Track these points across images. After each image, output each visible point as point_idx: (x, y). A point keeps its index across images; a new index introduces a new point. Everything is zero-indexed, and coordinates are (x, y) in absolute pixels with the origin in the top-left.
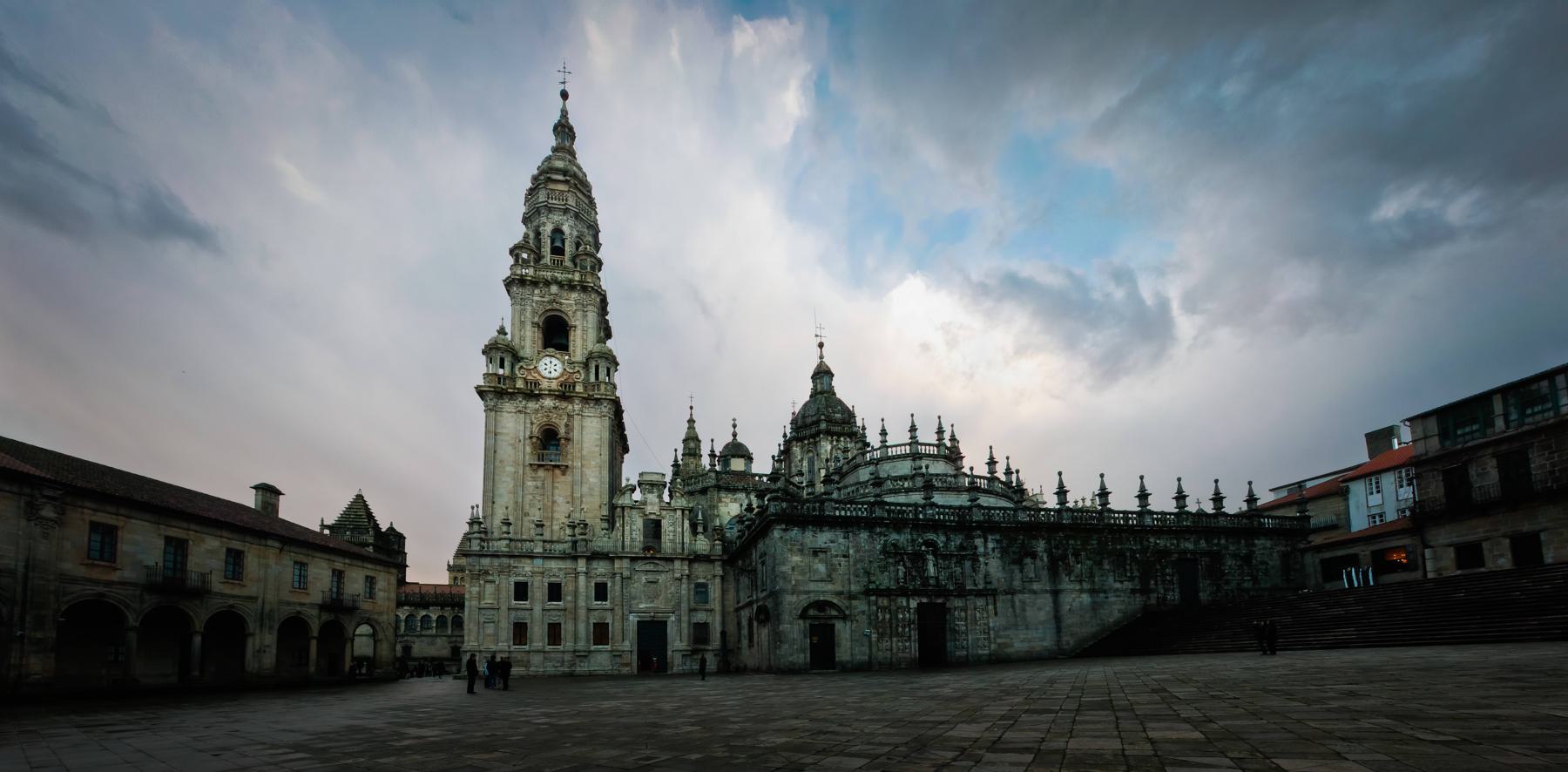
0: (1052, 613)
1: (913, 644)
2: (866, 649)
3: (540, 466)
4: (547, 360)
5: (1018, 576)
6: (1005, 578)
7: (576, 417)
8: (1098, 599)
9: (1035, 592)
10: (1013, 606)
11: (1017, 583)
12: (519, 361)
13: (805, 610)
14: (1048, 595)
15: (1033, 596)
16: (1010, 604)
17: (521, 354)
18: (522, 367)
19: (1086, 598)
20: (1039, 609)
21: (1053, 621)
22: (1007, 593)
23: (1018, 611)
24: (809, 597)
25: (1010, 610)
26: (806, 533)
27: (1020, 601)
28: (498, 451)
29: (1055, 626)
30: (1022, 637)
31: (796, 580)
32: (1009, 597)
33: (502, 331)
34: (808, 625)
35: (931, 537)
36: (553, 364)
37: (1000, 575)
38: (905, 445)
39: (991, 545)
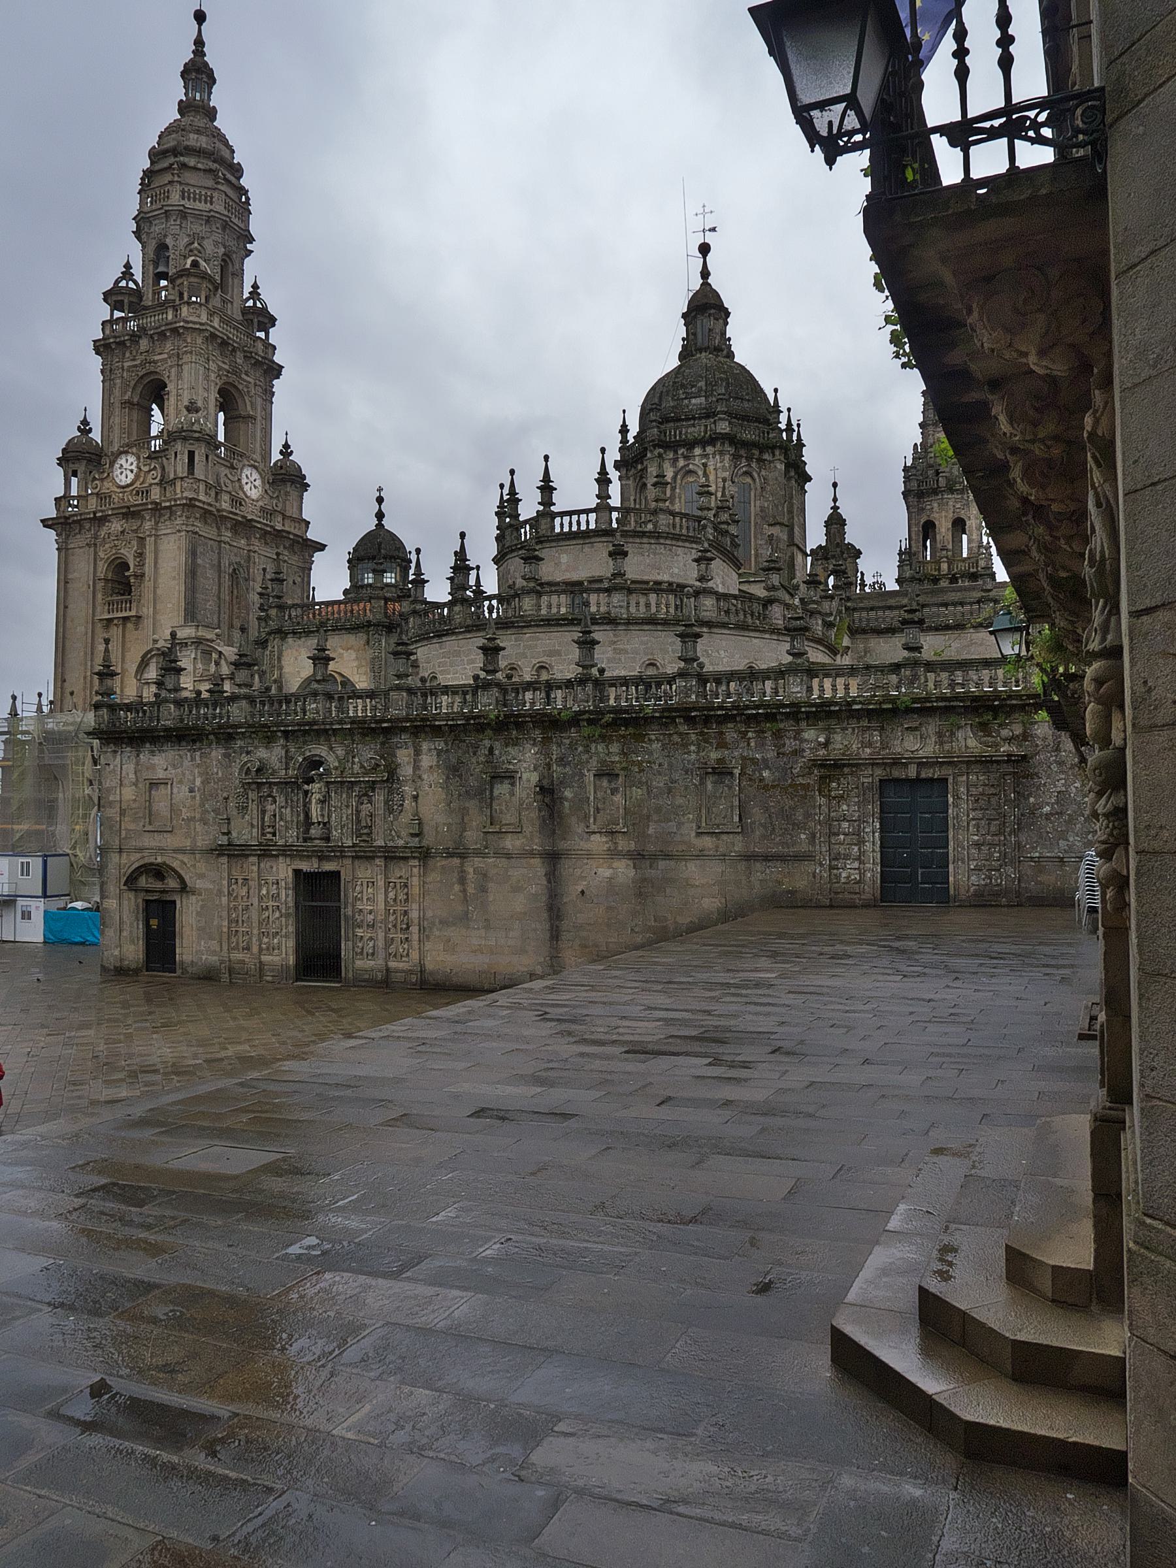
3: (110, 620)
6: (449, 825)
7: (148, 539)
8: (651, 873)
9: (508, 856)
10: (462, 881)
11: (472, 837)
14: (537, 861)
15: (503, 862)
16: (455, 876)
19: (624, 870)
20: (516, 889)
21: (545, 915)
22: (451, 855)
23: (471, 890)
24: (143, 857)
25: (457, 887)
28: (70, 606)
30: (475, 941)
32: (456, 861)
34: (140, 901)
37: (440, 818)
38: (587, 511)
39: (427, 761)
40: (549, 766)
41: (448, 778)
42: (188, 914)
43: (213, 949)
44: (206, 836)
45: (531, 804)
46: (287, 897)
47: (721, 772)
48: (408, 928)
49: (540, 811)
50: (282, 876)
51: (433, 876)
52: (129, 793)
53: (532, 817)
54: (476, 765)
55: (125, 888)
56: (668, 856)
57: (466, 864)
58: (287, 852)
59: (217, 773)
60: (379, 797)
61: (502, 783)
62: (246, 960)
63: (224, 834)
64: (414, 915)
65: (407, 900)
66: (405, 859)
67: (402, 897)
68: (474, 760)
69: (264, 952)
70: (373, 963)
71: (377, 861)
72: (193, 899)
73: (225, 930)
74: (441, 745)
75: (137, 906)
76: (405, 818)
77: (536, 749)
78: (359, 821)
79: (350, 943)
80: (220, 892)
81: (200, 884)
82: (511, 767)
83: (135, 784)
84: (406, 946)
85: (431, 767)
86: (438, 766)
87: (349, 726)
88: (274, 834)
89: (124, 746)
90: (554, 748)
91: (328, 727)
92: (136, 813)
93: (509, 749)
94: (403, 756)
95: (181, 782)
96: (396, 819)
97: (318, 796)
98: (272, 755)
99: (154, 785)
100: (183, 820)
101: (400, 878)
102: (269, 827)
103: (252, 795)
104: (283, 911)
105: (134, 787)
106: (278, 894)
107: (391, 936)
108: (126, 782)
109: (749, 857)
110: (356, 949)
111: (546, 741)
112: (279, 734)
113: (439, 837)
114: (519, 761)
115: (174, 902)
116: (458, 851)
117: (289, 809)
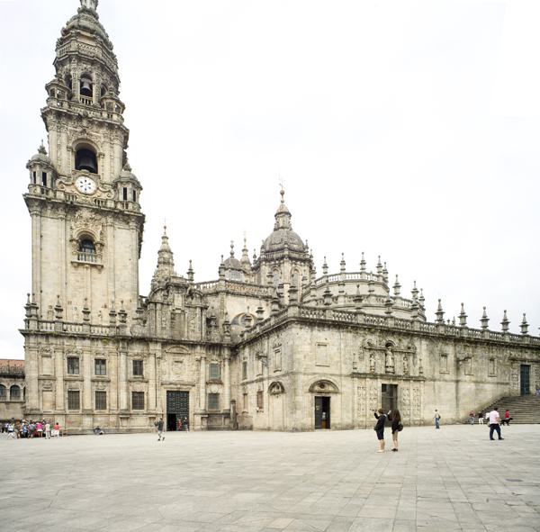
0: (455, 395)
2: (350, 415)
4: (82, 179)
5: (437, 369)
9: (446, 381)
11: (437, 375)
12: (58, 178)
13: (313, 386)
17: (59, 171)
18: (61, 182)
33: (42, 150)
36: (88, 182)
37: (429, 368)
42: (335, 402)
44: (347, 370)
46: (379, 393)
47: (492, 360)
53: (452, 369)
54: (437, 350)
56: (483, 383)
58: (382, 376)
60: (411, 358)
72: (339, 396)
81: (344, 389)
83: (310, 344)
94: (417, 344)
98: (374, 339)
103: (367, 354)
109: (498, 383)
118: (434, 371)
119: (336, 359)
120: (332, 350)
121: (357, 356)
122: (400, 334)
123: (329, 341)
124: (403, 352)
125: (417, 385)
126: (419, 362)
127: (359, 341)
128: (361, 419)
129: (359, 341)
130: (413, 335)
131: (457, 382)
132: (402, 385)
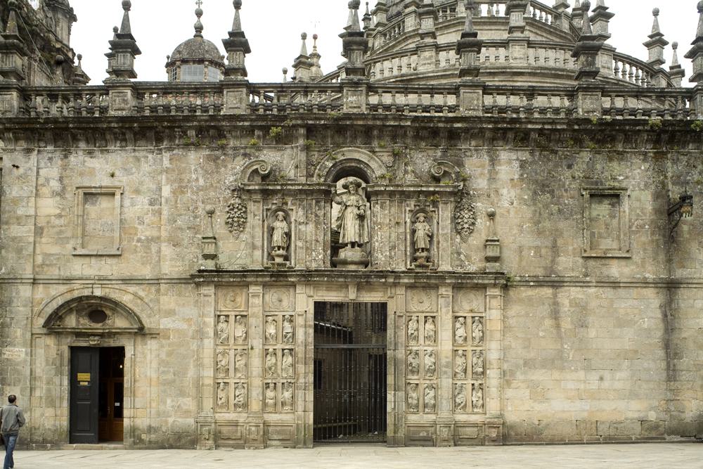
0: (659, 334)
1: (300, 393)
2: (189, 403)
5: (572, 243)
6: (537, 249)
9: (615, 285)
10: (555, 315)
11: (568, 264)
14: (650, 293)
15: (609, 293)
22: (539, 283)
23: (566, 324)
25: (548, 323)
26: (72, 158)
27: (574, 303)
29: (664, 365)
31: (47, 255)
32: (548, 291)
35: (356, 156)
37: (528, 240)
40: (664, 185)
41: (535, 193)
43: (185, 408)
45: (642, 227)
48: (483, 373)
49: (653, 234)
50: (300, 309)
51: (514, 310)
52: (49, 206)
53: (643, 242)
55: (45, 331)
57: (559, 295)
59: (197, 180)
60: (445, 213)
61: (600, 202)
62: (241, 420)
63: (206, 257)
64: (493, 355)
65: (482, 339)
66: (484, 287)
67: (477, 334)
68: (568, 173)
69: (269, 409)
70: (433, 417)
71: (442, 290)
72: (152, 344)
73: (209, 381)
74: (525, 155)
75: (61, 356)
76: (476, 240)
77: (647, 165)
78: (413, 243)
79: (401, 394)
80: (200, 334)
81: (165, 323)
82: (616, 184)
83: (61, 194)
84: (480, 394)
85: (512, 180)
86: (521, 179)
87: (409, 123)
88: (287, 258)
89: (42, 144)
90: (669, 164)
91: (378, 123)
92: (61, 232)
93: (615, 164)
95: (137, 192)
96: (464, 240)
97: (356, 211)
99: (90, 195)
100: (139, 240)
101: (471, 311)
102: (279, 248)
103: (256, 210)
104: (301, 355)
105: (58, 198)
106: (294, 334)
107: (459, 383)
108: (45, 190)
110: (410, 401)
111: (659, 156)
112: (302, 131)
113: (524, 263)
114: (627, 177)
115: (121, 351)
116: (548, 279)
117: (311, 227)
118: (555, 250)
119: (144, 232)
120: (137, 207)
121: (220, 219)
122: (396, 134)
123: (122, 179)
124: (405, 195)
125: (470, 303)
126: (482, 223)
127: (233, 170)
128: (231, 416)
129: (233, 170)
130: (453, 136)
131: (671, 287)
132: (398, 302)
